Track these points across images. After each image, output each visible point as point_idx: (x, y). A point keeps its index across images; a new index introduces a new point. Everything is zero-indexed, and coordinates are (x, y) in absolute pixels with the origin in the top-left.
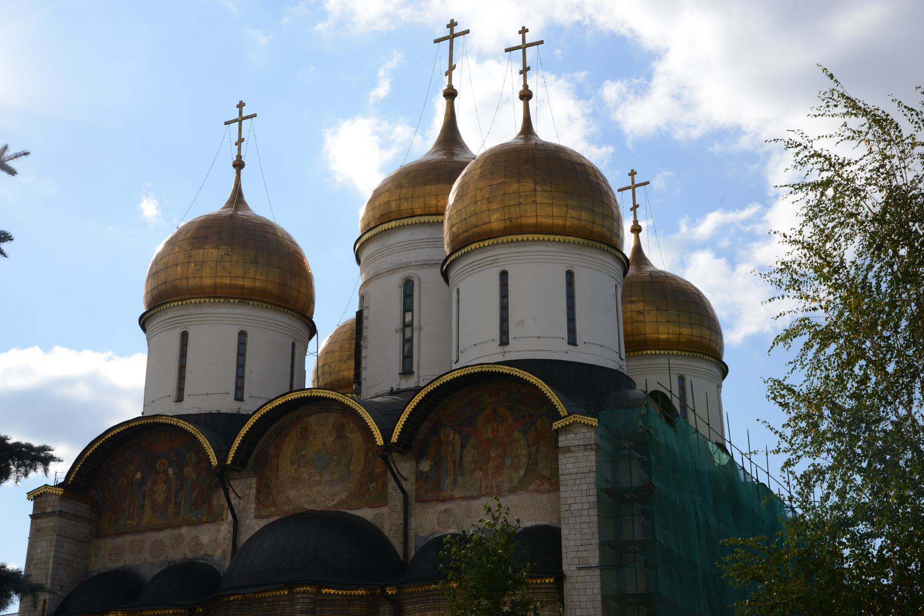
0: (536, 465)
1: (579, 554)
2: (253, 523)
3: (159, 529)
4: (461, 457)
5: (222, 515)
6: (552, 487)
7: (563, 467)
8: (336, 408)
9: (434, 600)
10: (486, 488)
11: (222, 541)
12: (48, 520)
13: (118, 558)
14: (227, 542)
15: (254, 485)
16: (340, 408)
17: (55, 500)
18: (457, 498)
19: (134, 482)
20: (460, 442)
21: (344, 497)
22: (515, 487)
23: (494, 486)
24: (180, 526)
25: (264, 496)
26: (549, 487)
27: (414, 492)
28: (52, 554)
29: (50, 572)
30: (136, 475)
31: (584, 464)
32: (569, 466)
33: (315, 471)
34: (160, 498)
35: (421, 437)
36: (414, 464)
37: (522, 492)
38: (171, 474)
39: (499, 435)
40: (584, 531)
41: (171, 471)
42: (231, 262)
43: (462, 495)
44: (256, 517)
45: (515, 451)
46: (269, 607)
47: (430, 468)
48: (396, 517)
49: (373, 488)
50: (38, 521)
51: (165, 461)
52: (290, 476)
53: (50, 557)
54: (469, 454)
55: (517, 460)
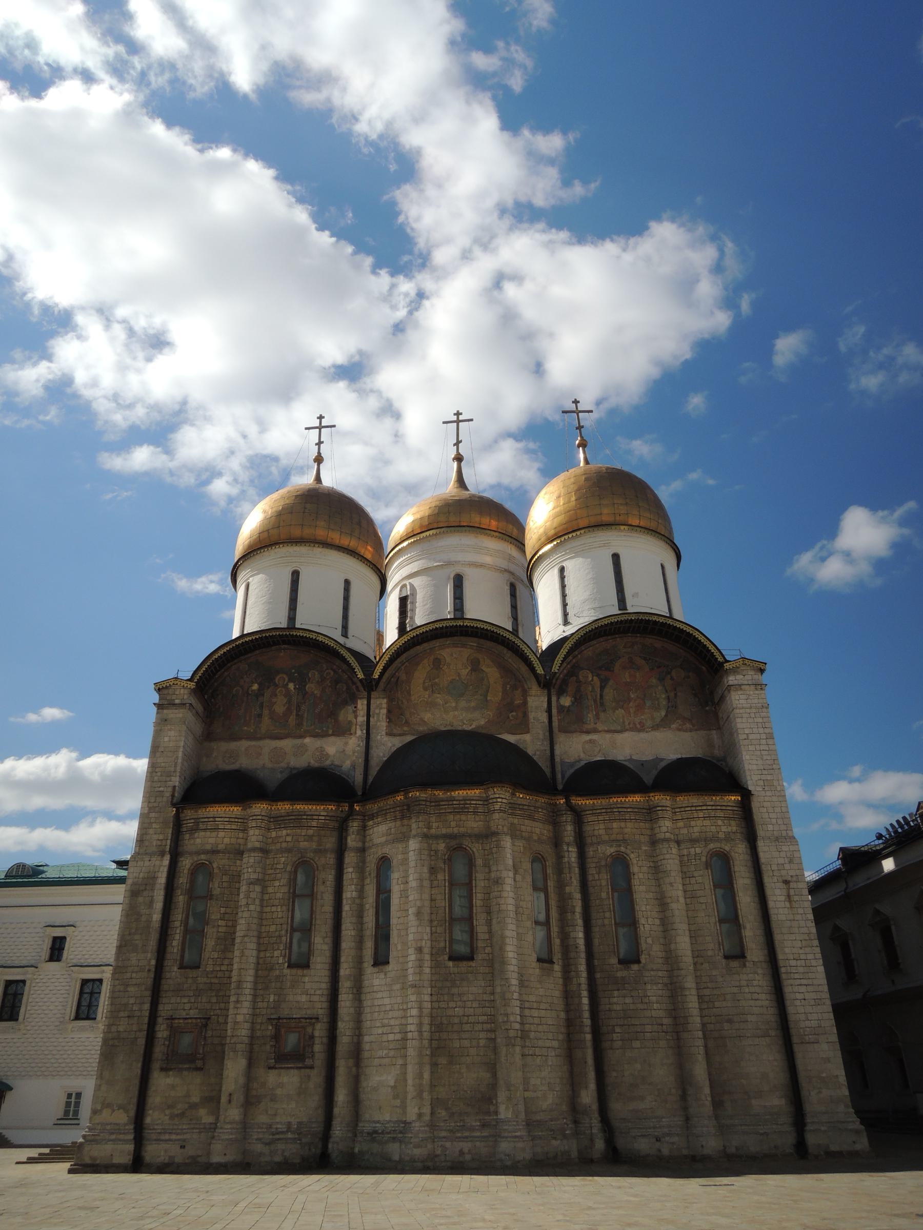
1: (764, 777)
2: (385, 739)
4: (601, 696)
5: (350, 730)
6: (694, 725)
7: (737, 702)
8: (471, 644)
10: (629, 724)
11: (351, 754)
12: (177, 711)
14: (356, 754)
15: (385, 706)
16: (475, 645)
17: (184, 694)
19: (250, 693)
20: (599, 683)
21: (483, 723)
25: (395, 715)
26: (691, 727)
28: (182, 744)
29: (180, 761)
30: (252, 686)
31: (756, 701)
33: (450, 698)
34: (280, 709)
38: (292, 689)
40: (765, 757)
41: (291, 686)
43: (606, 729)
44: (387, 734)
47: (571, 704)
48: (539, 743)
50: (165, 711)
51: (285, 676)
53: (180, 747)
54: (609, 693)
55: (657, 702)
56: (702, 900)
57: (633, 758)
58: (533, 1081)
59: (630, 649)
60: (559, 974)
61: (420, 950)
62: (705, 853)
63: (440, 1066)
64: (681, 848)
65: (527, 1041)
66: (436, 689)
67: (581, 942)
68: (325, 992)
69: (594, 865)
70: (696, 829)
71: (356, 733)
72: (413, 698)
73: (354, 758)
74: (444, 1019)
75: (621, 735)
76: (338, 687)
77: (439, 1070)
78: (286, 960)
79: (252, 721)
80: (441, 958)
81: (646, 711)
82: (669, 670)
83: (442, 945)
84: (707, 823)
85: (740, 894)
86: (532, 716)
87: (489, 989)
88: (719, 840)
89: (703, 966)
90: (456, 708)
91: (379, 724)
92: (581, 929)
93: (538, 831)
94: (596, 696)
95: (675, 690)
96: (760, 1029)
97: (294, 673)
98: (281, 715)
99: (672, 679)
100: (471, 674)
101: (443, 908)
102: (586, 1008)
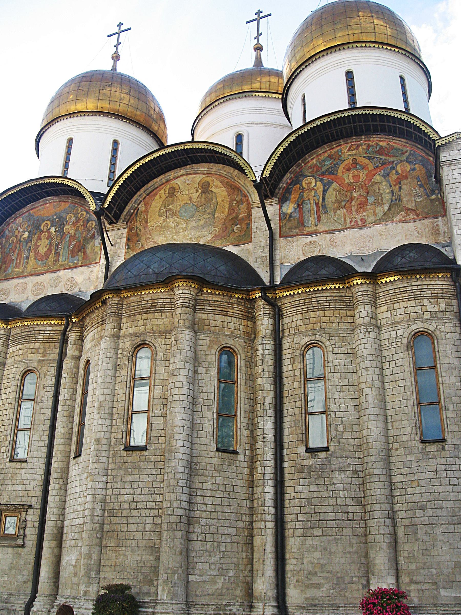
0: (399, 200)
3: (42, 274)
4: (324, 199)
5: (95, 260)
6: (418, 215)
7: (450, 177)
8: (202, 169)
9: (318, 301)
10: (351, 222)
11: (94, 280)
13: (6, 297)
14: (99, 280)
15: (125, 235)
16: (206, 169)
18: (322, 232)
19: (22, 240)
20: (322, 187)
21: (209, 239)
22: (379, 219)
23: (358, 220)
24: (58, 270)
26: (415, 217)
27: (279, 230)
32: (454, 176)
33: (182, 220)
34: (42, 250)
35: (285, 185)
36: (277, 207)
37: (387, 223)
38: (53, 232)
39: (361, 180)
41: (53, 230)
42: (111, 91)
43: (327, 229)
45: (377, 191)
46: (148, 305)
47: (293, 210)
49: (237, 229)
51: (48, 222)
52: (158, 226)
54: (331, 195)
55: (380, 197)
56: (400, 383)
57: (353, 254)
58: (199, 566)
59: (354, 151)
60: (245, 465)
61: (98, 441)
62: (406, 335)
63: (108, 548)
64: (382, 332)
65: (196, 527)
66: (170, 214)
67: (270, 433)
68: (41, 483)
69: (289, 356)
70: (400, 311)
71: (99, 262)
72: (149, 224)
73: (97, 284)
74: (116, 504)
75: (341, 234)
76: (88, 225)
77: (108, 552)
78: (9, 455)
79: (22, 263)
80: (118, 449)
81: (368, 207)
82: (394, 165)
83: (120, 436)
84: (412, 303)
85: (444, 374)
86: (254, 226)
87: (159, 477)
88: (423, 320)
89: (398, 452)
90: (186, 229)
91: (119, 251)
92: (272, 419)
93: (231, 326)
94: (318, 200)
95: (400, 183)
96: (457, 516)
97: (56, 219)
98: (43, 255)
99: (397, 173)
100: (202, 196)
101: (124, 401)
102: (271, 496)
